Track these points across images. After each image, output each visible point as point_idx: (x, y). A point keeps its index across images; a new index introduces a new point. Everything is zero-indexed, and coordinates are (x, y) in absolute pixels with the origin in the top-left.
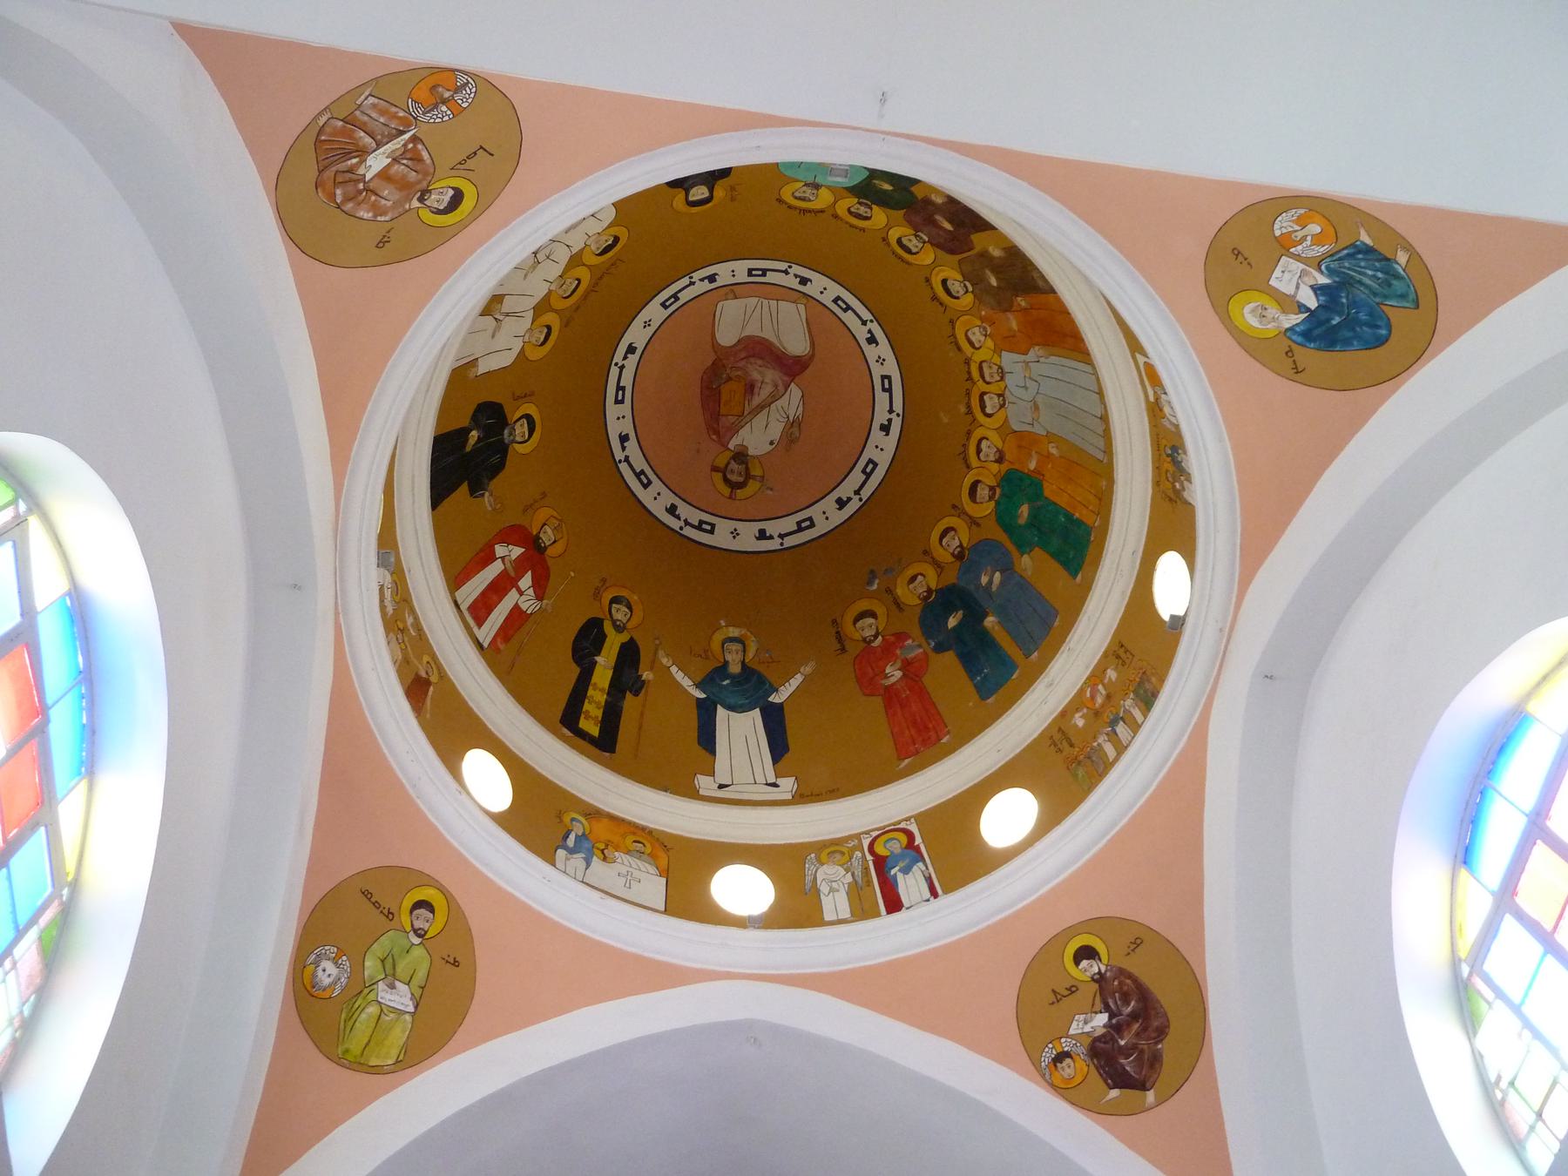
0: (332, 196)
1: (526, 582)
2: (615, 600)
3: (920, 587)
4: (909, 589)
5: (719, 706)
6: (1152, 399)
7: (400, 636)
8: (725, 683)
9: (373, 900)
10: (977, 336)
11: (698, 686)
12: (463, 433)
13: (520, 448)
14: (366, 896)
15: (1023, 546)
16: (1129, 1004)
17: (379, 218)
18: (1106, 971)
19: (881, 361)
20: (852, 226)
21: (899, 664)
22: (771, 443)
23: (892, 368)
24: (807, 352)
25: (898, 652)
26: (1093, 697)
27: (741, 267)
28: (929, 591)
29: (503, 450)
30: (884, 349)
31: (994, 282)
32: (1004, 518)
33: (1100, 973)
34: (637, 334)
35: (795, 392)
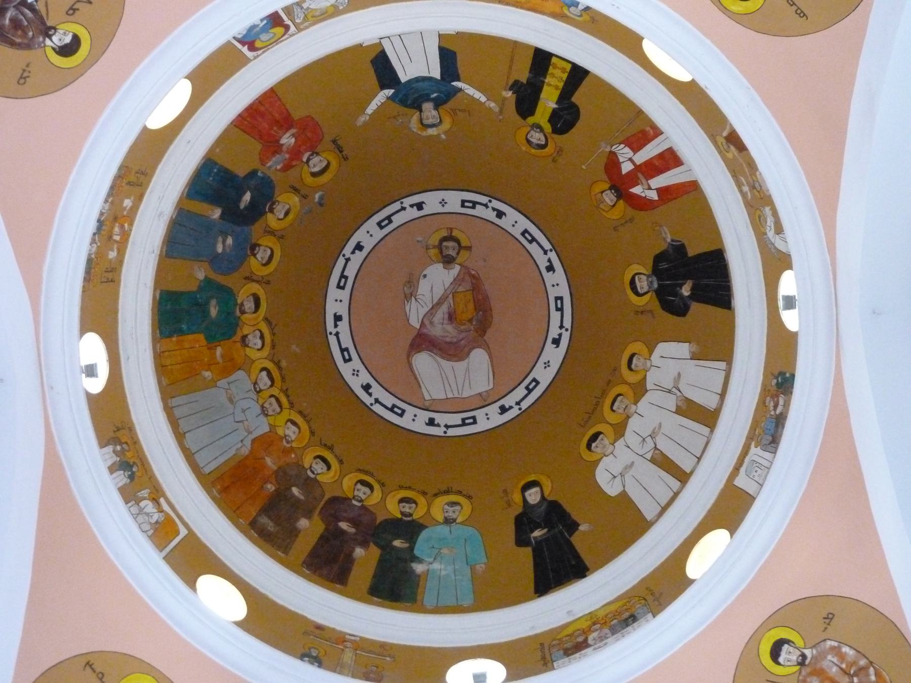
0: (877, 674)
1: (626, 168)
2: (543, 147)
3: (280, 211)
4: (289, 204)
5: (440, 79)
6: (162, 500)
7: (757, 185)
8: (435, 95)
9: (794, 8)
10: (291, 431)
11: (460, 90)
12: (695, 296)
13: (643, 270)
14: (802, 12)
15: (208, 281)
16: (11, 20)
17: (836, 644)
18: (44, 40)
19: (356, 373)
20: (409, 488)
21: (284, 148)
22: (425, 276)
23: (346, 370)
24: (414, 358)
25: (287, 156)
26: (122, 226)
27: (483, 425)
28: (271, 210)
29: (656, 271)
30: (356, 384)
31: (295, 490)
32: (226, 295)
33: (50, 37)
34: (554, 356)
35: (415, 322)
